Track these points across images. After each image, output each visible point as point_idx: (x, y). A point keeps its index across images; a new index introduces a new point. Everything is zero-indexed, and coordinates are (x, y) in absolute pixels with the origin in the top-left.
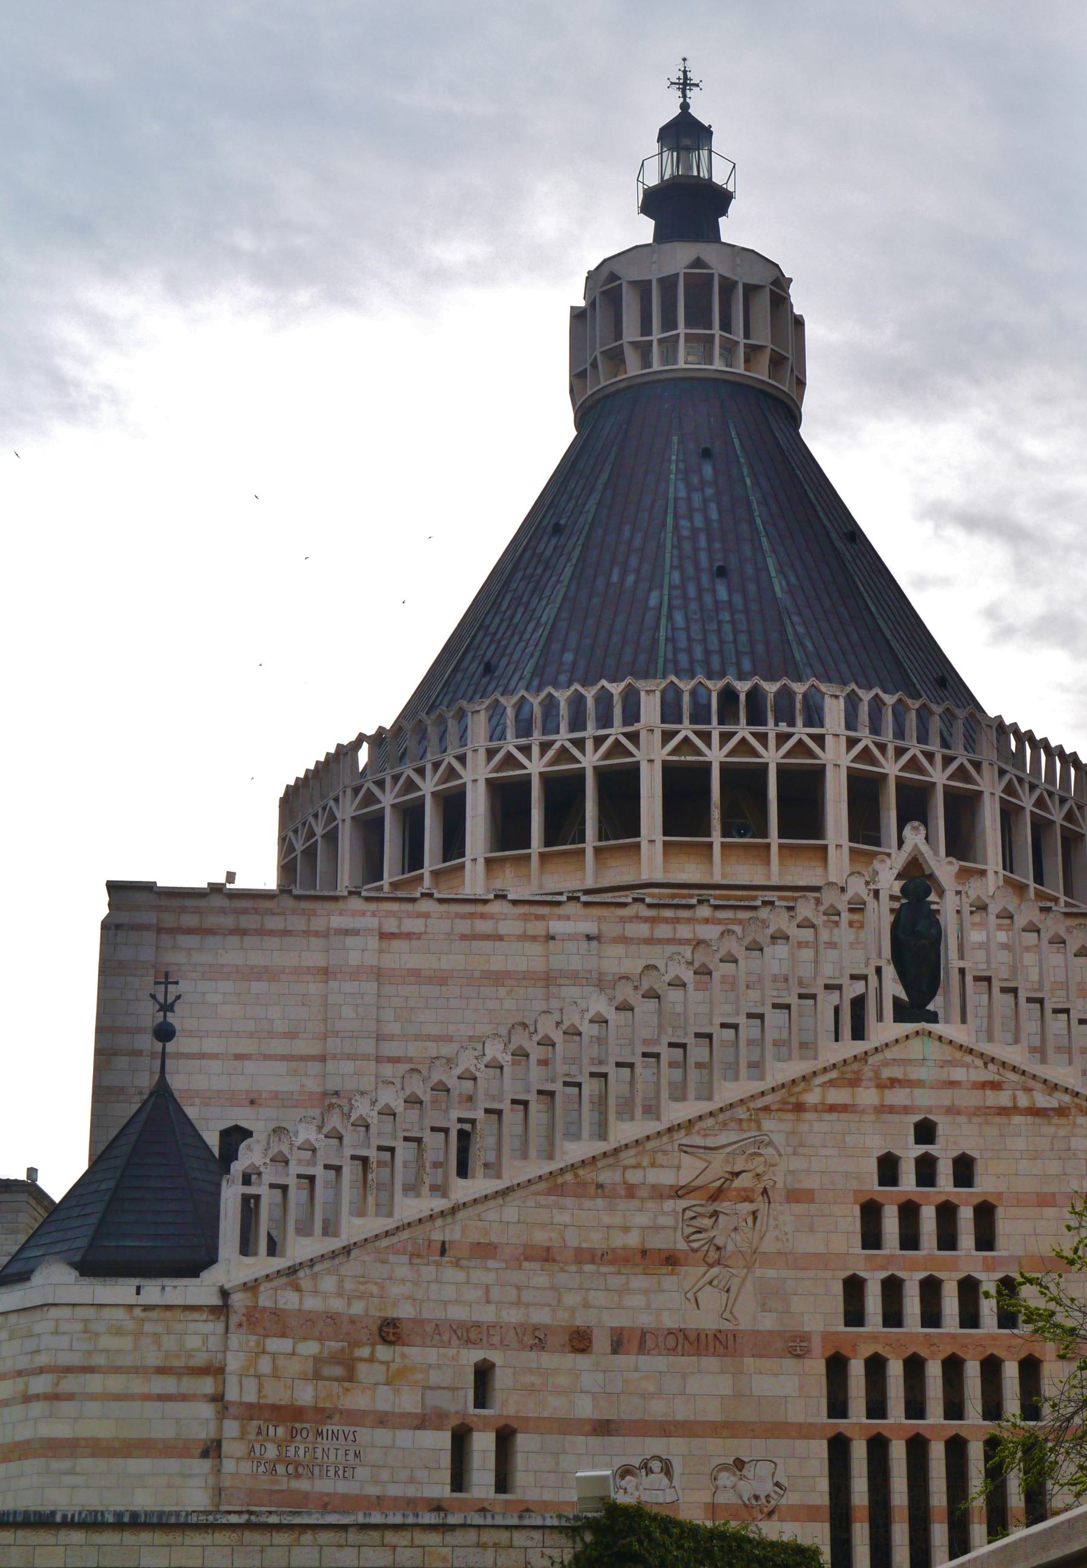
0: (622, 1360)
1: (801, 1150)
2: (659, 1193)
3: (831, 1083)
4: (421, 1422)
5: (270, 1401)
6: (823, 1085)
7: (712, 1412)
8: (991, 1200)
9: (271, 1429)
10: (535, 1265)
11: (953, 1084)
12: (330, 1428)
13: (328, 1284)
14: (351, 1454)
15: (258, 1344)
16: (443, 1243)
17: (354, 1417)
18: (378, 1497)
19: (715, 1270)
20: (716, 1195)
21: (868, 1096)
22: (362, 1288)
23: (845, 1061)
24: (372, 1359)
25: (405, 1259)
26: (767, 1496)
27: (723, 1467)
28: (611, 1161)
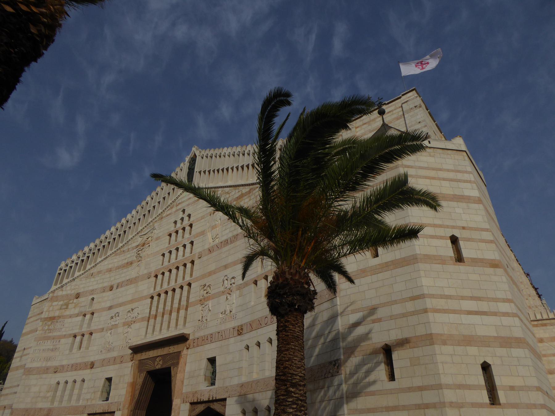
0: (118, 290)
1: (161, 228)
2: (133, 249)
3: (168, 210)
4: (77, 315)
5: (49, 316)
6: (167, 211)
7: (130, 298)
8: (192, 223)
9: (48, 322)
10: (108, 273)
11: (190, 198)
12: (59, 320)
13: (68, 288)
14: (62, 325)
15: (51, 305)
16: (93, 273)
17: (64, 317)
18: (65, 335)
19: (139, 262)
20: (144, 245)
21: (174, 209)
22: (75, 287)
23: (171, 203)
24: (73, 303)
25: (85, 279)
26: (136, 317)
27: (129, 311)
28: (127, 244)
